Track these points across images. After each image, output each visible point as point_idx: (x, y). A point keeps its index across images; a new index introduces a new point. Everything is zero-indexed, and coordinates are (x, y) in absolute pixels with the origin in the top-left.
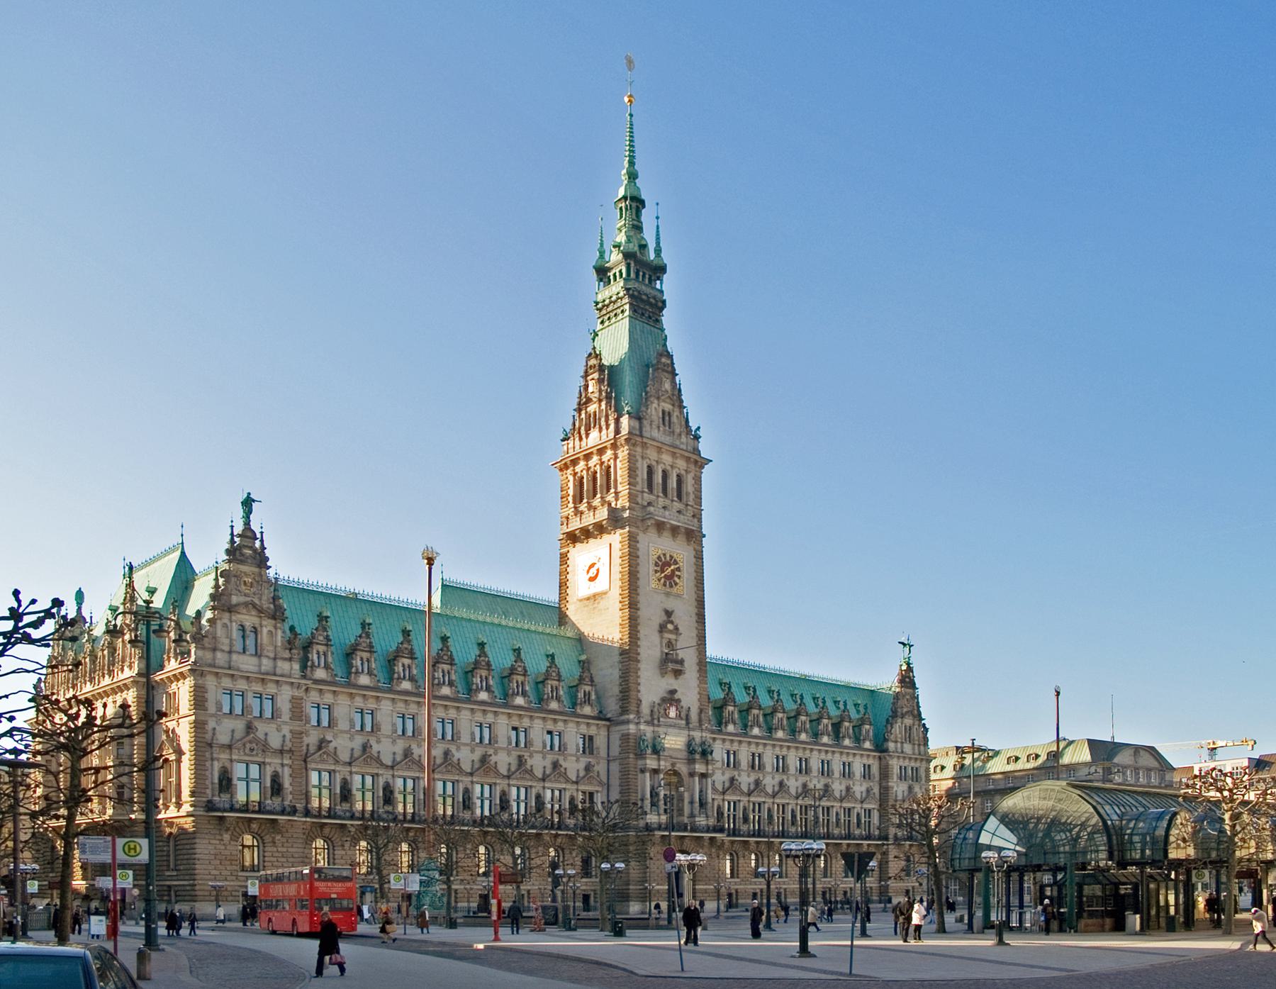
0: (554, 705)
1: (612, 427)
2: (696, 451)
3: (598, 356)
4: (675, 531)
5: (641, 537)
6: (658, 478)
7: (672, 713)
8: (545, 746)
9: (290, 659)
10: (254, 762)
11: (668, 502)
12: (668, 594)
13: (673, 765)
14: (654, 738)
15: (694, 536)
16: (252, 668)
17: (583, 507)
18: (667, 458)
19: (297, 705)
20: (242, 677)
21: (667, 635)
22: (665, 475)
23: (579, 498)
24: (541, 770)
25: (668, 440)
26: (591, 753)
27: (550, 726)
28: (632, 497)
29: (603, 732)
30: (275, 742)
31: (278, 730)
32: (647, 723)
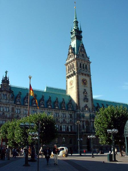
0: (64, 108)
1: (73, 57)
2: (89, 61)
3: (71, 46)
4: (85, 75)
5: (79, 76)
6: (82, 65)
7: (87, 109)
8: (62, 116)
9: (12, 100)
10: (4, 121)
11: (84, 70)
12: (85, 86)
13: (87, 120)
14: (83, 114)
15: (89, 76)
16: (5, 102)
17: (69, 71)
18: (83, 62)
19: (13, 109)
20: (3, 104)
21: (85, 94)
22: (83, 65)
23: (69, 70)
24: (61, 121)
25: (83, 59)
26: (71, 118)
27: (63, 112)
28: (77, 69)
29: (74, 114)
30: (8, 116)
31: (9, 114)
32: (82, 111)
